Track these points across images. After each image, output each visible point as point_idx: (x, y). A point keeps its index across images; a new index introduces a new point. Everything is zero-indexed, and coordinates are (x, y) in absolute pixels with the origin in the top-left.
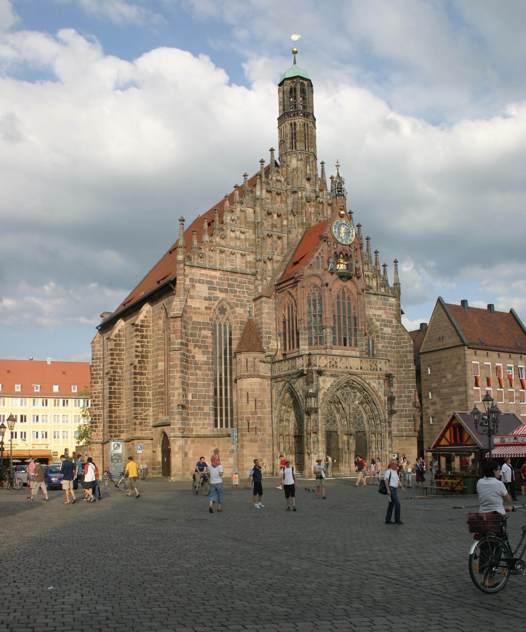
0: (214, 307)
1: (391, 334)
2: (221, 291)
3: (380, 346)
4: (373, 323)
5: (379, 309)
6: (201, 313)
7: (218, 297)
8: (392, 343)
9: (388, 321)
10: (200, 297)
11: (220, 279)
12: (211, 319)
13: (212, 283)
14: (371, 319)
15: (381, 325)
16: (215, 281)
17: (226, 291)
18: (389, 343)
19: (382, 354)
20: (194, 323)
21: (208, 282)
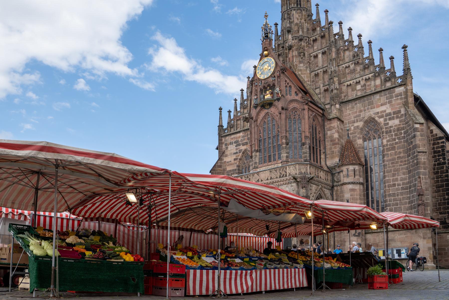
0: (239, 158)
1: (400, 125)
2: (243, 145)
3: (385, 141)
4: (376, 121)
5: (382, 105)
6: (231, 164)
7: (242, 150)
8: (401, 134)
9: (394, 113)
10: (231, 154)
11: (243, 137)
12: (238, 166)
13: (238, 141)
14: (374, 119)
15: (385, 120)
16: (240, 140)
17: (246, 143)
18: (396, 135)
19: (387, 149)
20: (228, 172)
21: (235, 142)
